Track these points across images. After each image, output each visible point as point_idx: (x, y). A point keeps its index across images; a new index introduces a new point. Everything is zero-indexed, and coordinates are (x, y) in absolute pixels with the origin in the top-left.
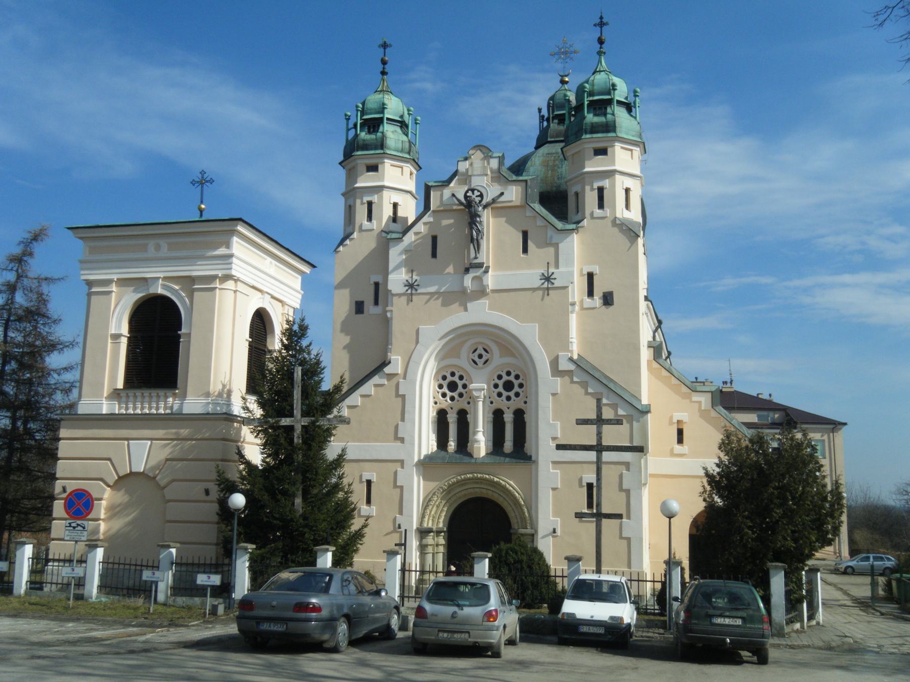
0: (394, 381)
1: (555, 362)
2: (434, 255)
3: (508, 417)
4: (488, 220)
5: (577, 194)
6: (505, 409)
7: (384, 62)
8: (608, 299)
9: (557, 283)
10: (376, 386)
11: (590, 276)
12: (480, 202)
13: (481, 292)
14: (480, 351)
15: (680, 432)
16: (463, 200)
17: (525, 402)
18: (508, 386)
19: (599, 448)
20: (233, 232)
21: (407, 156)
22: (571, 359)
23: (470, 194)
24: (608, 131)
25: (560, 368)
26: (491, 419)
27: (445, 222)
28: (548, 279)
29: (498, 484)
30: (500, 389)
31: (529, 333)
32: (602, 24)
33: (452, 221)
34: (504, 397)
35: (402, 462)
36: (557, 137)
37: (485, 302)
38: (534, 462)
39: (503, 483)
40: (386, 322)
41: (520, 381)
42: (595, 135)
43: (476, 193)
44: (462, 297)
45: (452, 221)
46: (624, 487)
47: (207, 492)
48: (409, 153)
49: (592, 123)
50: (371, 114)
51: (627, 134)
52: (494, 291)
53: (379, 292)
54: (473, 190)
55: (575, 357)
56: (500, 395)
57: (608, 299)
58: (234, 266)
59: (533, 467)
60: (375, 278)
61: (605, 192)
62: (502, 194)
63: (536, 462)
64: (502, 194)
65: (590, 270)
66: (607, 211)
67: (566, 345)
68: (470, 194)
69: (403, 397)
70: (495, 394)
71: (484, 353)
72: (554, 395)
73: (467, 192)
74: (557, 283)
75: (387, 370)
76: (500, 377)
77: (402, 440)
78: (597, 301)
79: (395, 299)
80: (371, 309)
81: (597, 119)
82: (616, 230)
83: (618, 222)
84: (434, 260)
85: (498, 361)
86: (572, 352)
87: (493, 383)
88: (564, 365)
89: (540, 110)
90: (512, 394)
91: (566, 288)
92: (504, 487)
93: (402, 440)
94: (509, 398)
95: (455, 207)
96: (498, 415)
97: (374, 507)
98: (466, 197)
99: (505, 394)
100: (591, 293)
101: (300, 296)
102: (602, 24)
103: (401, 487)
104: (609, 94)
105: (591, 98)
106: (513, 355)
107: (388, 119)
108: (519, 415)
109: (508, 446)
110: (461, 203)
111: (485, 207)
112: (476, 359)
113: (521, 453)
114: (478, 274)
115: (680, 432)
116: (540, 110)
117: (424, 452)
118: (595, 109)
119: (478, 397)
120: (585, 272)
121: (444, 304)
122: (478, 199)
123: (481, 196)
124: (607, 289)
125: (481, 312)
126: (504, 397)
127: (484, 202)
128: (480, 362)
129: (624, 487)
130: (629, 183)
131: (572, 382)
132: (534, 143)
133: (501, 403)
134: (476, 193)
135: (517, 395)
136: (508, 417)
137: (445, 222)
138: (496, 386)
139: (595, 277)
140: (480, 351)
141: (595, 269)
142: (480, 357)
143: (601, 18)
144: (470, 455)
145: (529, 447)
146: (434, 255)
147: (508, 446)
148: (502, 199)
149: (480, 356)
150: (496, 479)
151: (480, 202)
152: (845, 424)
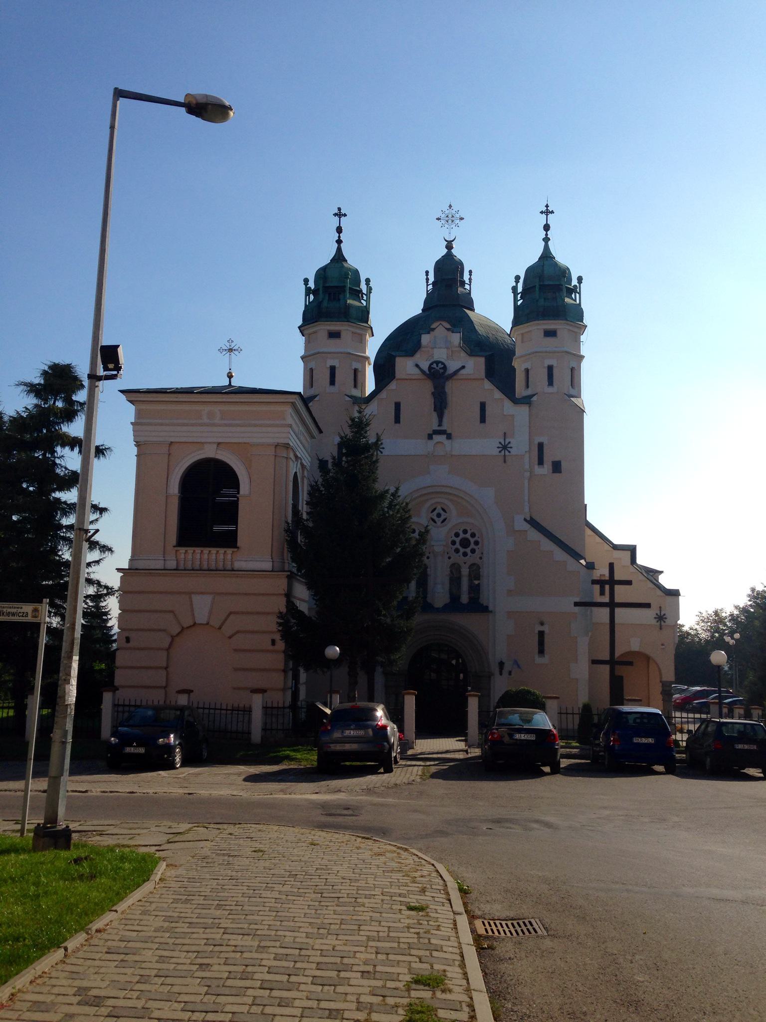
3: (465, 571)
6: (462, 564)
8: (557, 467)
9: (514, 451)
11: (541, 446)
17: (481, 558)
18: (465, 543)
23: (435, 366)
25: (517, 528)
30: (458, 545)
32: (547, 212)
43: (440, 366)
47: (273, 642)
55: (528, 519)
62: (463, 367)
64: (463, 367)
68: (435, 366)
71: (442, 512)
73: (432, 364)
78: (547, 468)
89: (427, 273)
90: (468, 550)
94: (465, 554)
98: (430, 368)
99: (462, 550)
100: (541, 462)
112: (435, 518)
116: (427, 273)
120: (536, 443)
122: (442, 371)
133: (458, 558)
134: (440, 366)
135: (473, 551)
136: (465, 571)
138: (454, 543)
140: (439, 510)
143: (547, 206)
148: (463, 372)
149: (439, 515)
152: (662, 572)
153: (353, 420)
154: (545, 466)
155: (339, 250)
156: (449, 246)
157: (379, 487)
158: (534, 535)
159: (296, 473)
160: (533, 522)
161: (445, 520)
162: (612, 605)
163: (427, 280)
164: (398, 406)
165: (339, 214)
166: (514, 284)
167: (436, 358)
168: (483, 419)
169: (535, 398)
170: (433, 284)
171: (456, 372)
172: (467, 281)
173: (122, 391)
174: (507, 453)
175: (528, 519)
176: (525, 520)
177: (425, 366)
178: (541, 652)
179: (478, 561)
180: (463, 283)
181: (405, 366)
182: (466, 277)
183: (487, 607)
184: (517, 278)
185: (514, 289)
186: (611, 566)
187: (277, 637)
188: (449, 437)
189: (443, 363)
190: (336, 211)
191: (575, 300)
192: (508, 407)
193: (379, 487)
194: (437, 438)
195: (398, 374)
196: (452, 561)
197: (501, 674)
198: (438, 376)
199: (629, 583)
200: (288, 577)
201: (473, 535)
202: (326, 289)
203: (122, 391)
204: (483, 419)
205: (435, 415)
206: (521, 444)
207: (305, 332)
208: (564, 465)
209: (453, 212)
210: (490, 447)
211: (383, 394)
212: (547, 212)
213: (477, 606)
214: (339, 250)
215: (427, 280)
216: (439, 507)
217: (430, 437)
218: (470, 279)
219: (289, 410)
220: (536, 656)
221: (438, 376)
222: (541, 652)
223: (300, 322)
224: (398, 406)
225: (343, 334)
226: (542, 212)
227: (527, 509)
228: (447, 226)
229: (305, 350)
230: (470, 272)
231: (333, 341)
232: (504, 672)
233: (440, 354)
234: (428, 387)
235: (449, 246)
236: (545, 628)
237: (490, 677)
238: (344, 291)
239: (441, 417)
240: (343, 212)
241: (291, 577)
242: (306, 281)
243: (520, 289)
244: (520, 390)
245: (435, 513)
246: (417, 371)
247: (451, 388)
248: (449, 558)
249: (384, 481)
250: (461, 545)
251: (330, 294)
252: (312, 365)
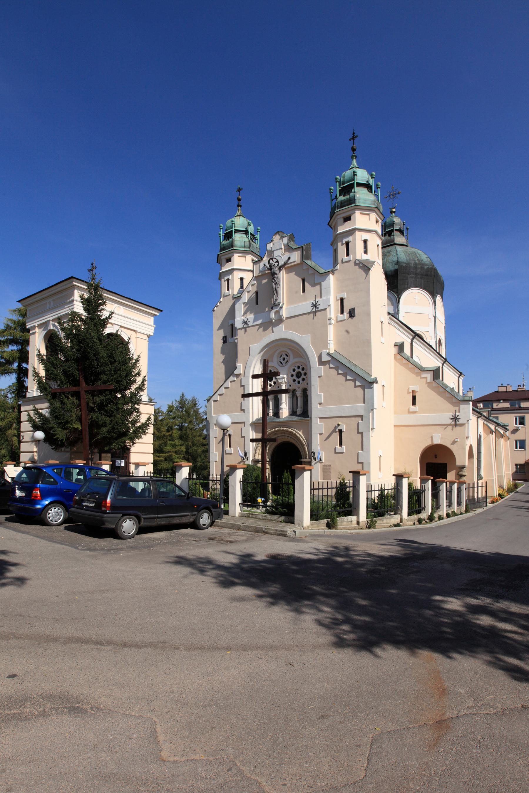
0: (239, 378)
1: (320, 357)
2: (257, 304)
3: (299, 393)
4: (283, 277)
6: (297, 389)
7: (239, 200)
8: (352, 314)
9: (321, 308)
10: (231, 382)
12: (278, 265)
13: (280, 320)
15: (414, 398)
18: (299, 375)
20: (74, 287)
21: (248, 249)
22: (329, 354)
27: (264, 281)
28: (315, 305)
29: (292, 433)
30: (295, 377)
31: (306, 341)
32: (354, 138)
33: (266, 280)
34: (296, 382)
35: (244, 423)
37: (283, 325)
39: (294, 432)
40: (236, 345)
41: (305, 371)
43: (275, 260)
44: (268, 325)
45: (266, 280)
46: (360, 431)
48: (249, 248)
51: (364, 203)
52: (287, 318)
53: (233, 330)
56: (294, 381)
57: (352, 314)
58: (75, 306)
60: (230, 322)
61: (350, 244)
62: (289, 258)
63: (311, 418)
64: (289, 258)
65: (341, 297)
66: (351, 256)
67: (326, 344)
69: (244, 386)
70: (292, 381)
72: (320, 377)
73: (269, 261)
74: (321, 308)
75: (236, 372)
77: (243, 410)
78: (346, 315)
79: (239, 332)
80: (229, 340)
82: (357, 267)
83: (357, 262)
86: (329, 349)
88: (325, 358)
90: (300, 379)
91: (325, 309)
92: (295, 434)
93: (243, 410)
95: (267, 272)
97: (232, 449)
99: (297, 380)
101: (153, 328)
102: (354, 138)
103: (244, 437)
106: (301, 357)
111: (280, 268)
112: (282, 361)
113: (305, 413)
114: (278, 309)
115: (414, 398)
117: (255, 417)
119: (282, 383)
120: (339, 298)
121: (264, 330)
123: (277, 261)
125: (282, 332)
126: (296, 382)
129: (360, 431)
130: (366, 236)
131: (330, 368)
135: (303, 380)
136: (299, 393)
137: (264, 281)
138: (292, 376)
141: (345, 295)
142: (284, 359)
143: (354, 133)
146: (257, 304)
147: (299, 411)
148: (290, 261)
149: (284, 359)
150: (290, 430)
171: (285, 264)
173: (19, 301)
201: (303, 369)
203: (19, 301)
216: (284, 354)
250: (301, 376)
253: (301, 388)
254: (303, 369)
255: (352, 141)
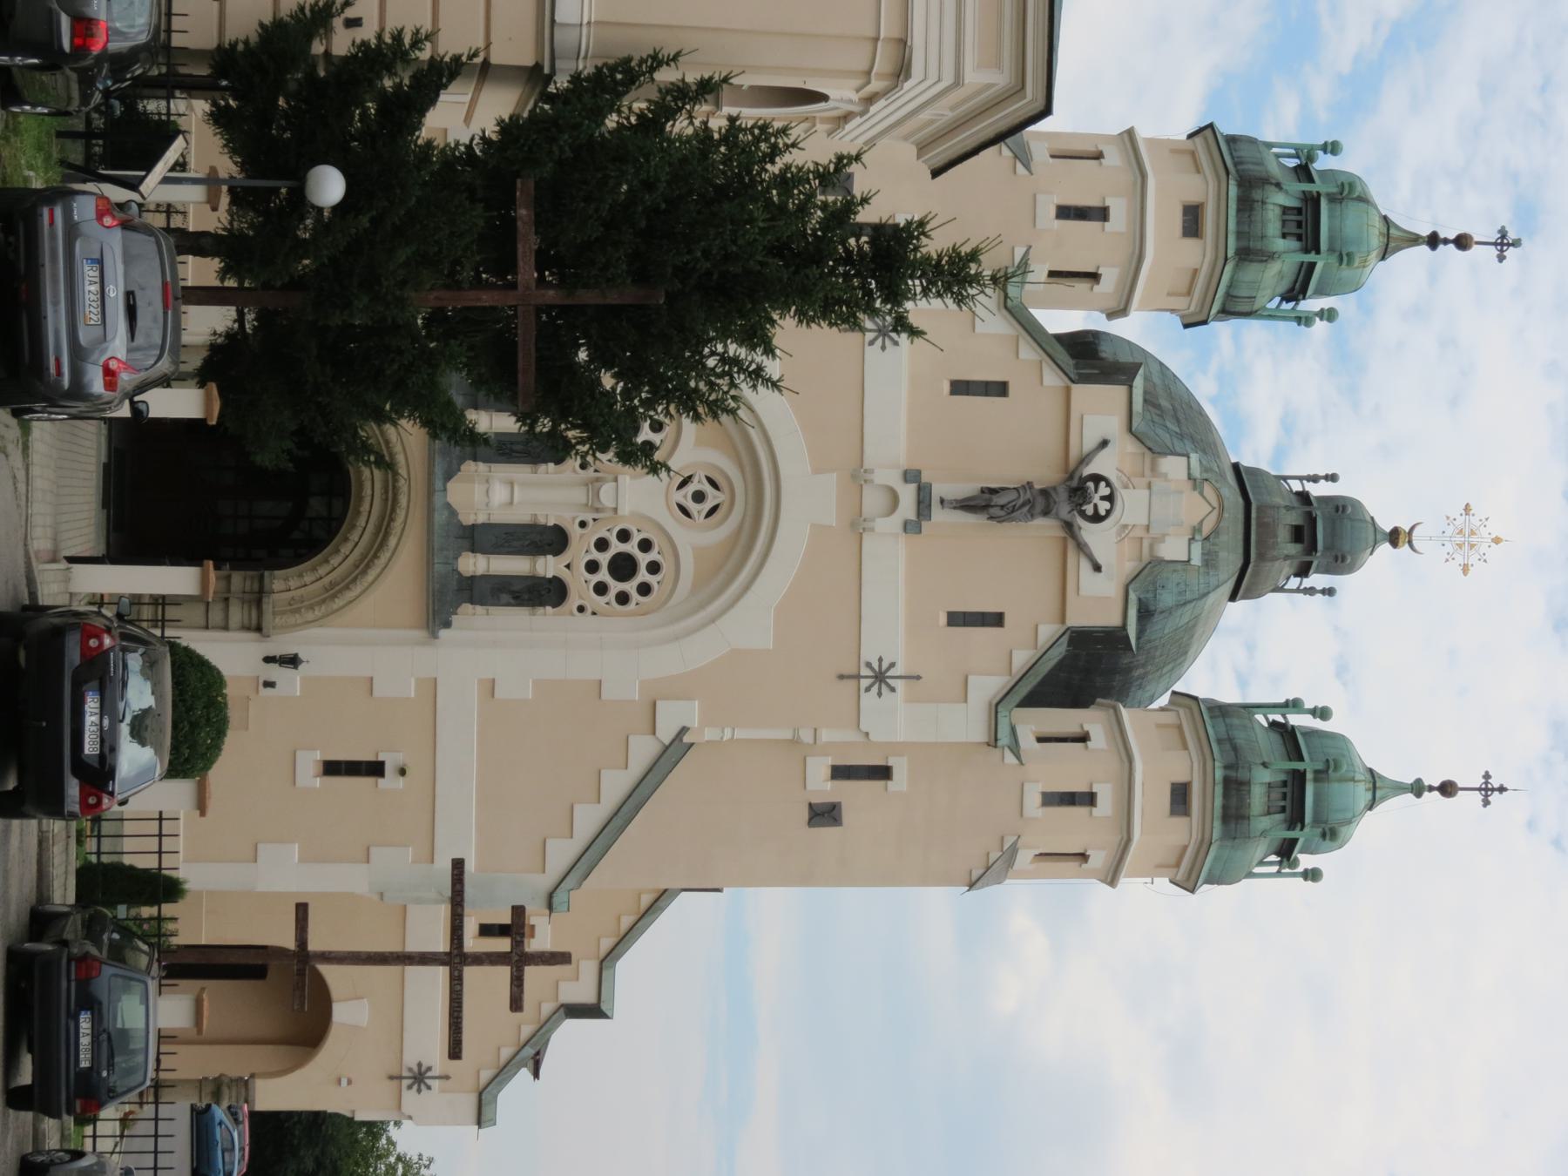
3: (548, 566)
5: (1083, 738)
8: (825, 814)
9: (869, 700)
11: (882, 773)
14: (713, 497)
16: (1088, 471)
17: (581, 609)
18: (623, 567)
19: (456, 959)
23: (1104, 490)
24: (1226, 818)
26: (542, 521)
30: (616, 547)
31: (752, 621)
34: (595, 555)
36: (1259, 525)
38: (434, 635)
42: (1219, 790)
43: (1104, 506)
49: (1248, 783)
50: (1331, 217)
54: (1110, 498)
55: (687, 739)
56: (602, 545)
57: (825, 814)
59: (421, 634)
68: (1104, 490)
70: (603, 534)
73: (1108, 484)
76: (646, 545)
78: (822, 787)
81: (1257, 798)
84: (946, 387)
85: (690, 543)
87: (633, 529)
89: (1332, 478)
90: (604, 575)
96: (554, 540)
98: (1097, 479)
99: (604, 559)
100: (841, 772)
104: (1317, 821)
105: (1309, 776)
107: (1312, 266)
108: (550, 593)
109: (474, 564)
110: (1085, 460)
111: (1069, 527)
112: (691, 488)
116: (1332, 478)
118: (1284, 784)
122: (1089, 509)
123: (1097, 518)
124: (847, 815)
127: (1080, 521)
128: (685, 496)
132: (1247, 462)
133: (581, 548)
134: (1104, 506)
135: (601, 589)
136: (548, 566)
138: (624, 536)
139: (882, 783)
140: (713, 497)
143: (1502, 789)
144: (449, 476)
145: (472, 621)
147: (474, 564)
148: (1085, 566)
149: (699, 497)
151: (1083, 514)
152: (536, 1075)
153: (974, 256)
154: (829, 785)
155: (1414, 240)
156: (1394, 537)
157: (786, 330)
158: (643, 750)
159: (822, 98)
160: (676, 750)
161: (685, 511)
162: (456, 959)
163: (1314, 479)
164: (1000, 389)
165: (1503, 243)
166: (1308, 705)
167: (1123, 495)
168: (958, 619)
169: (1010, 758)
170: (1304, 497)
171: (1082, 547)
172: (1308, 582)
174: (865, 683)
175: (687, 739)
176: (684, 730)
177: (1101, 465)
178: (332, 768)
179: (573, 601)
180: (1303, 571)
181: (1101, 411)
182: (1316, 580)
183: (448, 625)
184: (1323, 713)
185: (1294, 705)
186: (561, 958)
187: (367, 33)
188: (907, 526)
189: (1109, 512)
190: (1512, 236)
191: (1261, 863)
192: (988, 686)
193: (786, 330)
194: (908, 494)
195: (1082, 392)
196: (574, 531)
197: (268, 660)
198: (1073, 496)
199: (516, 1004)
200: (538, 67)
202: (1312, 201)
204: (958, 619)
205: (968, 489)
206: (890, 722)
207: (1198, 140)
208: (827, 833)
209: (1483, 548)
210: (888, 633)
211: (1029, 352)
212: (1487, 790)
213: (447, 598)
214: (1414, 240)
215: (1314, 479)
217: (911, 476)
218: (1311, 591)
219: (1001, 79)
220: (319, 756)
221: (1073, 496)
222: (332, 768)
223: (1226, 128)
224: (1000, 389)
225: (1191, 243)
226: (1487, 776)
227: (710, 734)
228: (1450, 530)
229: (1152, 142)
230: (1329, 592)
231: (1177, 220)
232: (274, 667)
233: (1132, 506)
234: (1044, 473)
235: (1394, 537)
236: (389, 781)
237: (259, 629)
238: (1306, 251)
239: (967, 505)
240: (1510, 252)
241: (536, 76)
242: (1333, 148)
243: (1295, 720)
244: (1033, 722)
245: (707, 488)
246: (1090, 443)
247: (1044, 529)
248: (583, 524)
249: (798, 342)
251: (1299, 211)
252: (1113, 158)
253: (565, 575)
254: (645, 589)
255: (1479, 782)
